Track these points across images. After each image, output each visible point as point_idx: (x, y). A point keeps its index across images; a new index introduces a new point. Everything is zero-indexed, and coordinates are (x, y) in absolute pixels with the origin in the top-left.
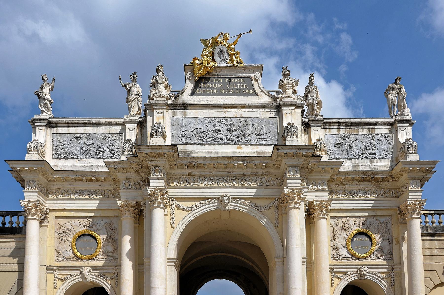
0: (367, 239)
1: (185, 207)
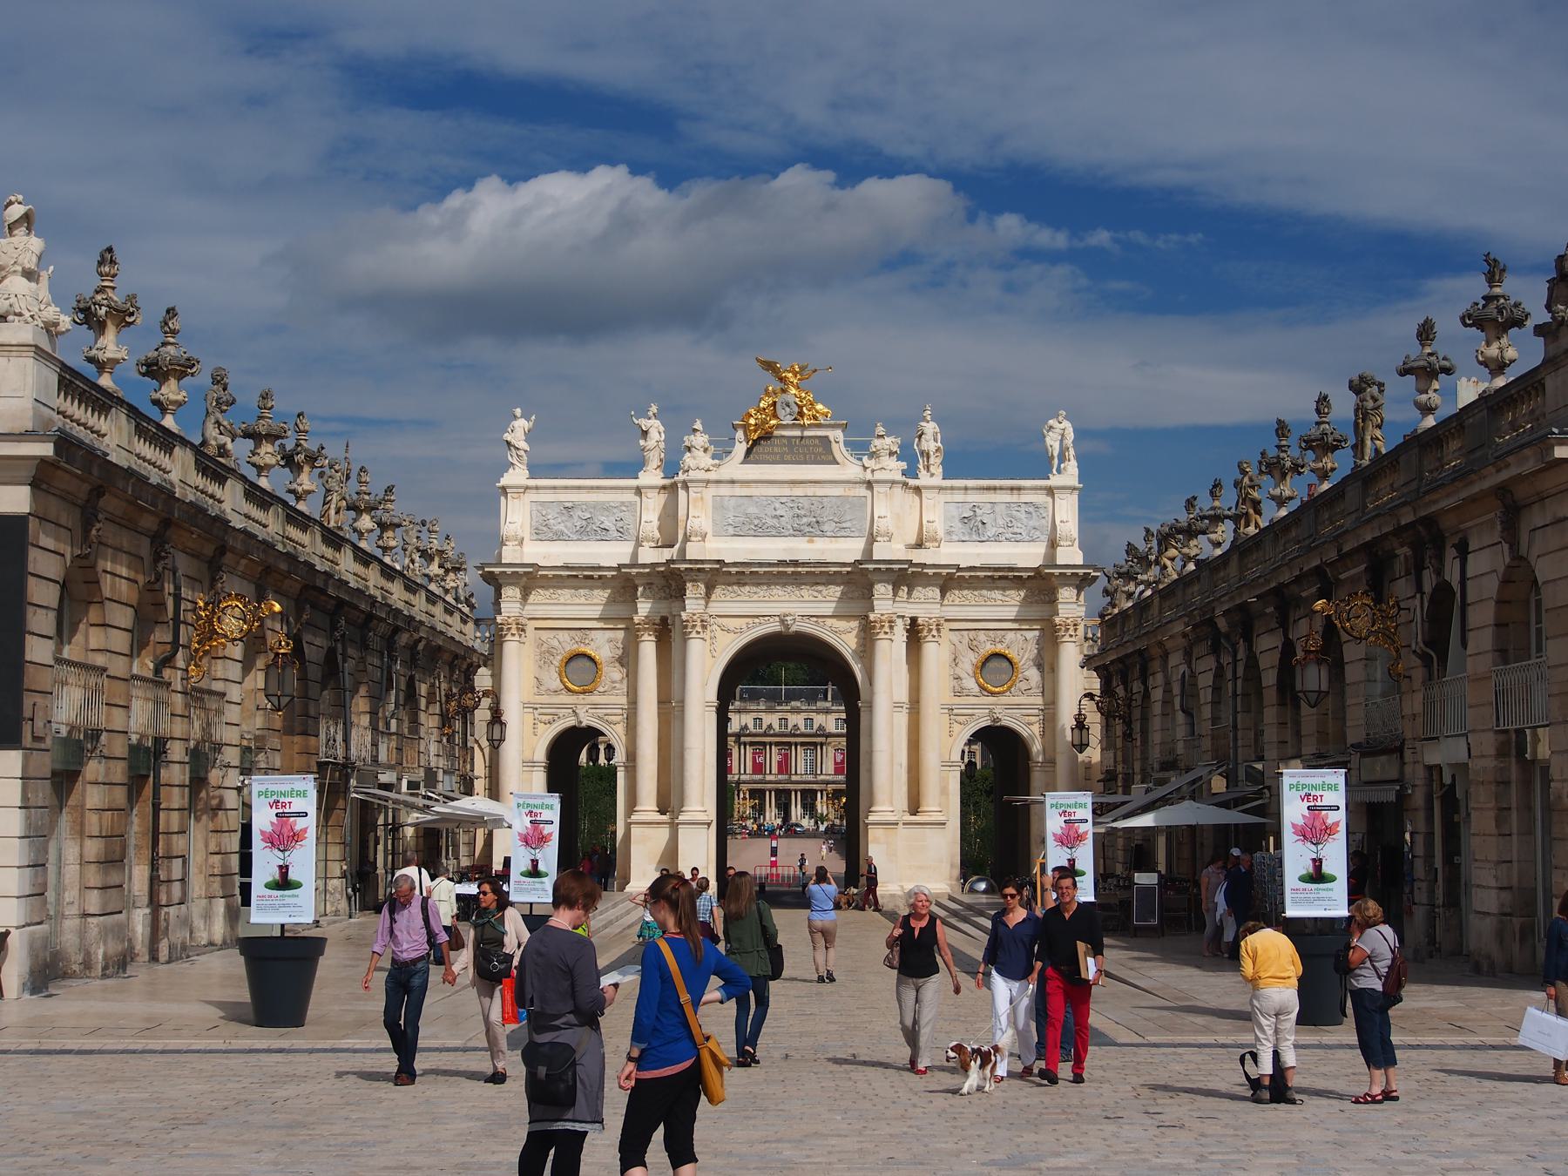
0: (1006, 664)
1: (732, 629)
